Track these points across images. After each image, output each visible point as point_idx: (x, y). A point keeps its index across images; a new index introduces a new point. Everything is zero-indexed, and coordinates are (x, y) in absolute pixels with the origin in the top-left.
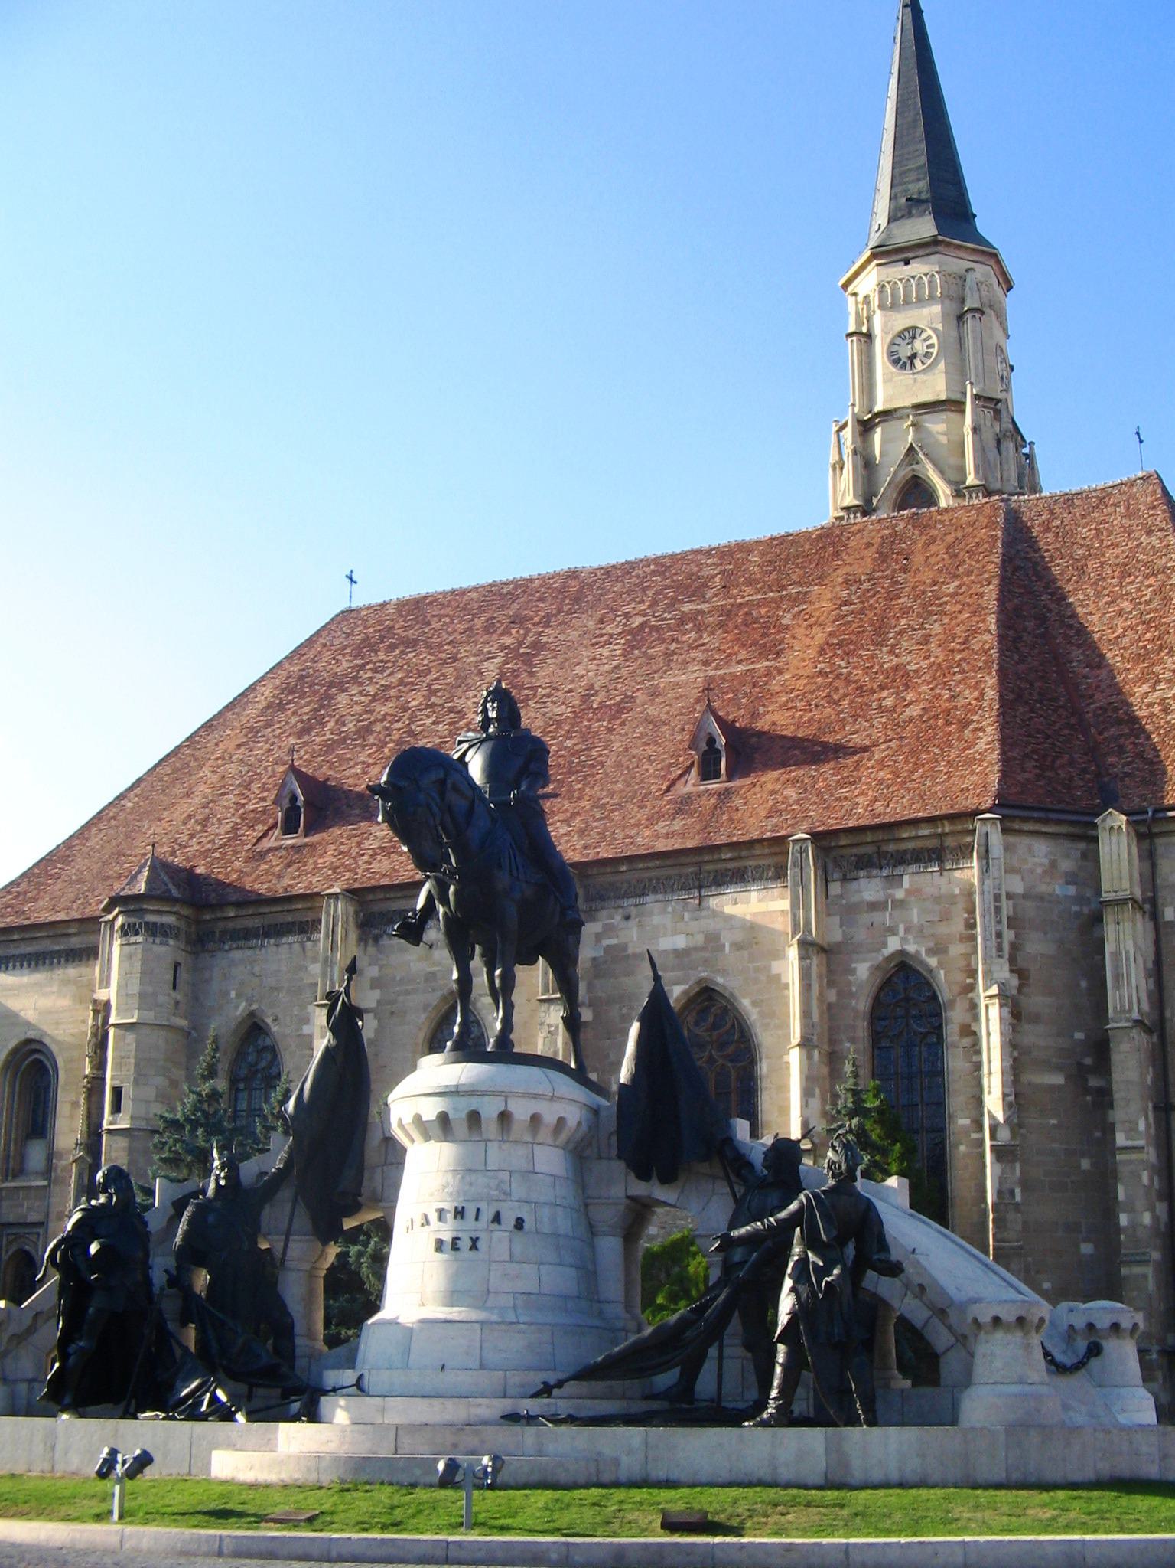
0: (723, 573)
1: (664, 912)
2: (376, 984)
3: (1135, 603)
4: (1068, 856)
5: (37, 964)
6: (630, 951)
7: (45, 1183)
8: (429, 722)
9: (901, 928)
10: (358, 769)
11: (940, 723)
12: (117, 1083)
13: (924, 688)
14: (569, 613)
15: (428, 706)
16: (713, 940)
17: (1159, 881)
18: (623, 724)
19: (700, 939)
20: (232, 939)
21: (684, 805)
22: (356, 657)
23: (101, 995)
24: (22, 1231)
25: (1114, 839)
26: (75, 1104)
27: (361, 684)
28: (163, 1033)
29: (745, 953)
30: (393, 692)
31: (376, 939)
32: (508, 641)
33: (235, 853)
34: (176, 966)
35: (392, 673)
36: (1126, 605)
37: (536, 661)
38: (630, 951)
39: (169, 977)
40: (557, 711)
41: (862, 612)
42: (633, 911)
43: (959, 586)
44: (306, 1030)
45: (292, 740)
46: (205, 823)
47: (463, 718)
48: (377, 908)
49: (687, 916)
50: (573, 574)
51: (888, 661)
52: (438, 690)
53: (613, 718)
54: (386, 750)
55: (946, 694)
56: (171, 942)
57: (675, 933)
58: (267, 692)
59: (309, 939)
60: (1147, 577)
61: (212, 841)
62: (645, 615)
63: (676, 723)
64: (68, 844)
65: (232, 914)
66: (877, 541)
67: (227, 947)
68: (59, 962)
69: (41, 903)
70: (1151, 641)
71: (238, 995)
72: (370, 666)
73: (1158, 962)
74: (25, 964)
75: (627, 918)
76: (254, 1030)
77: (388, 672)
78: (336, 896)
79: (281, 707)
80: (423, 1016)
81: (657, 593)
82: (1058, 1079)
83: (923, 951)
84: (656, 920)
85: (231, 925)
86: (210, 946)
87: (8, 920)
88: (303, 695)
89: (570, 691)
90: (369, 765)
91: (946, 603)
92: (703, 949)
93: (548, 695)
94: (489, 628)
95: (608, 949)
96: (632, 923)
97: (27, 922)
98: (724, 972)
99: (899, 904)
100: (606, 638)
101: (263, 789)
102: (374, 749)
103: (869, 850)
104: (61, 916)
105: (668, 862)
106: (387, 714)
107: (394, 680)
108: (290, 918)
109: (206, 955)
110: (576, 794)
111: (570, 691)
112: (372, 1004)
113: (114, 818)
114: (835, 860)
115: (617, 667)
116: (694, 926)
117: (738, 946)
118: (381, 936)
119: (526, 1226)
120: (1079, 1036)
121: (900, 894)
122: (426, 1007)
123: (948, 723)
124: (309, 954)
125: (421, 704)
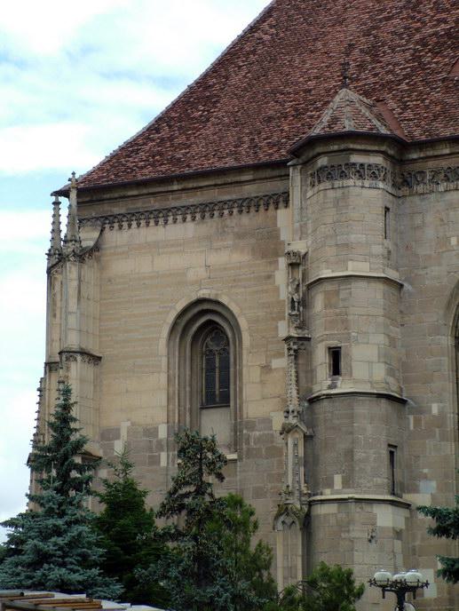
5: (203, 217)
12: (334, 343)
20: (447, 179)
23: (300, 246)
26: (266, 369)
28: (380, 286)
33: (426, 83)
34: (387, 209)
46: (374, 52)
56: (381, 185)
61: (391, 72)
65: (447, 151)
67: (441, 188)
68: (231, 213)
69: (195, 150)
74: (189, 217)
85: (444, 164)
86: (420, 188)
87: (163, 168)
97: (187, 171)
104: (230, 162)
109: (416, 199)
113: (254, 52)
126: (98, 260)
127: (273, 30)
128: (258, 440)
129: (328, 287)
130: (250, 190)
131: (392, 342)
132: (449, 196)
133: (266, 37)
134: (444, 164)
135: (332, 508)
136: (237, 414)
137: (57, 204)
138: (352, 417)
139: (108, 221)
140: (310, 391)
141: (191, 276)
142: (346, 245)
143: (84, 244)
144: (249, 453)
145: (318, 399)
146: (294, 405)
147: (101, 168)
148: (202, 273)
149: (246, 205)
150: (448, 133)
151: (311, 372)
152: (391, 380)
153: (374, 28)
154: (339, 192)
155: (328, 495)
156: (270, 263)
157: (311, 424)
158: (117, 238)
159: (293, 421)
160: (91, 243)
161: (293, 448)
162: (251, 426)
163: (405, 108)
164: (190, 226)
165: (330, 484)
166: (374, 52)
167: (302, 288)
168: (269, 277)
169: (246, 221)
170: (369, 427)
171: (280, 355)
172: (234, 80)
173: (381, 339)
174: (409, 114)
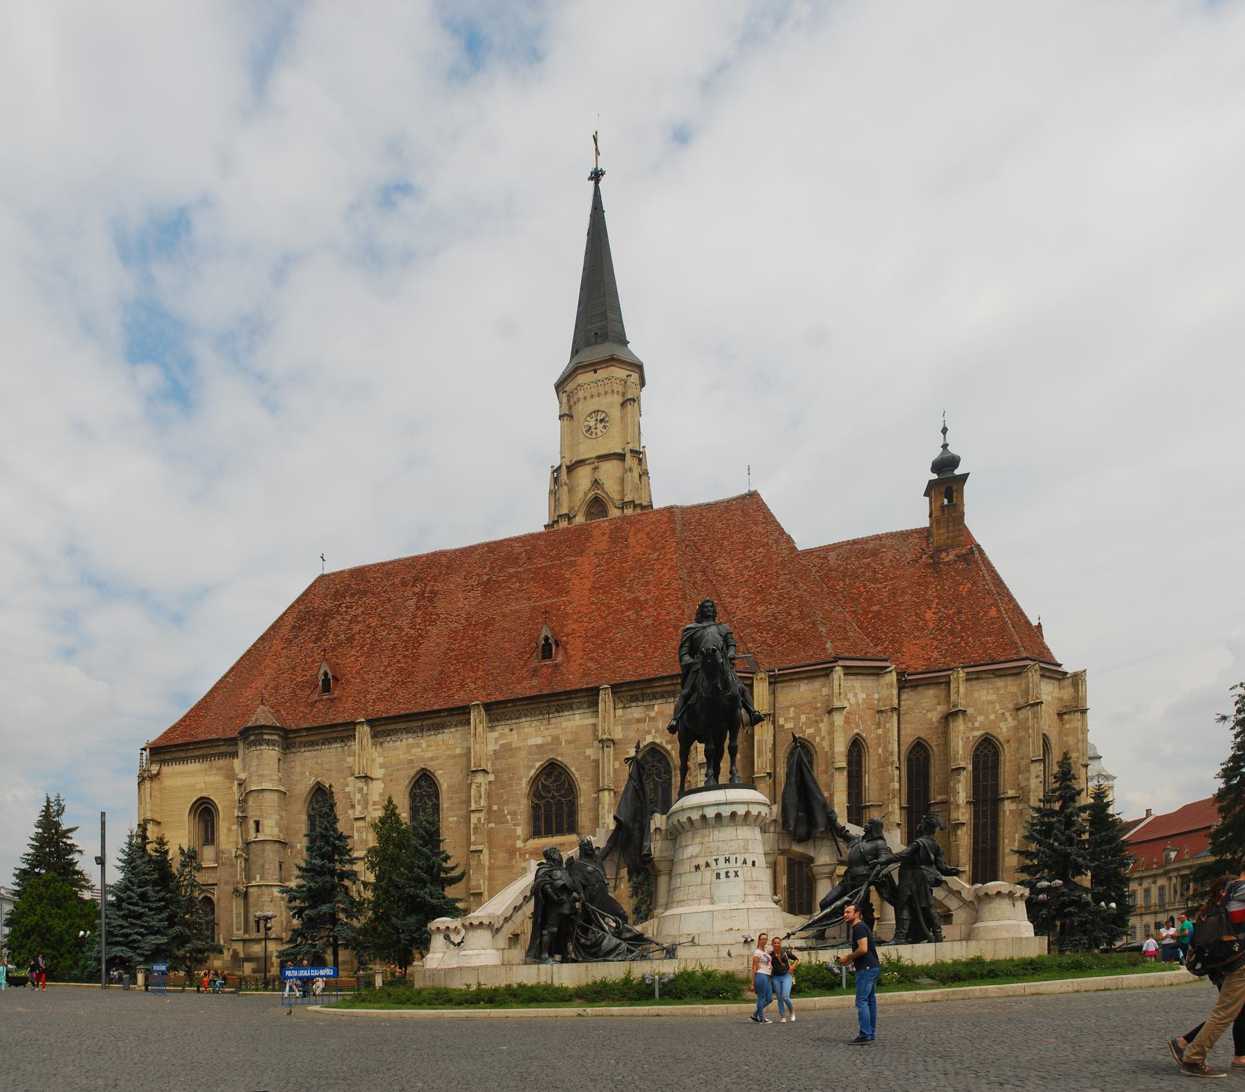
1: (530, 726)
2: (382, 766)
3: (754, 562)
6: (513, 746)
8: (384, 633)
9: (653, 731)
10: (353, 659)
12: (257, 819)
13: (651, 609)
15: (382, 626)
16: (556, 740)
18: (491, 632)
19: (549, 739)
20: (305, 746)
21: (535, 672)
22: (334, 601)
23: (243, 776)
26: (229, 830)
27: (342, 615)
29: (573, 745)
30: (360, 619)
31: (381, 744)
34: (279, 760)
36: (749, 563)
38: (513, 746)
39: (277, 766)
42: (514, 726)
44: (347, 789)
45: (312, 645)
47: (402, 631)
49: (542, 728)
52: (386, 617)
53: (486, 629)
55: (664, 612)
57: (536, 737)
58: (290, 620)
59: (346, 745)
60: (759, 548)
61: (283, 698)
71: (310, 774)
75: (511, 730)
77: (355, 608)
79: (301, 628)
83: (664, 742)
84: (526, 730)
86: (294, 750)
88: (310, 621)
90: (358, 657)
91: (654, 564)
95: (502, 745)
96: (513, 732)
98: (562, 755)
99: (653, 719)
101: (303, 670)
102: (358, 648)
104: (214, 736)
105: (534, 701)
108: (335, 735)
109: (292, 755)
110: (475, 669)
112: (382, 776)
113: (225, 687)
114: (619, 698)
116: (546, 733)
117: (568, 742)
118: (383, 742)
121: (653, 714)
122: (408, 777)
124: (346, 752)
125: (377, 624)
126: (159, 779)
129: (254, 794)
130: (223, 749)
131: (282, 818)
132: (305, 754)
133: (231, 681)
134: (304, 739)
137: (141, 754)
138: (264, 850)
139: (163, 762)
140: (247, 839)
141: (198, 787)
142: (262, 775)
143: (153, 772)
145: (250, 843)
146: (240, 846)
147: (160, 738)
148: (203, 786)
149: (221, 755)
150: (304, 726)
151: (247, 831)
152: (280, 834)
153: (276, 677)
157: (248, 854)
158: (167, 769)
159: (240, 852)
160: (156, 772)
161: (240, 864)
163: (288, 714)
164: (198, 764)
166: (276, 689)
167: (244, 795)
168: (231, 788)
169: (222, 762)
170: (271, 855)
171: (234, 824)
172: (217, 700)
173: (277, 817)
174: (290, 717)
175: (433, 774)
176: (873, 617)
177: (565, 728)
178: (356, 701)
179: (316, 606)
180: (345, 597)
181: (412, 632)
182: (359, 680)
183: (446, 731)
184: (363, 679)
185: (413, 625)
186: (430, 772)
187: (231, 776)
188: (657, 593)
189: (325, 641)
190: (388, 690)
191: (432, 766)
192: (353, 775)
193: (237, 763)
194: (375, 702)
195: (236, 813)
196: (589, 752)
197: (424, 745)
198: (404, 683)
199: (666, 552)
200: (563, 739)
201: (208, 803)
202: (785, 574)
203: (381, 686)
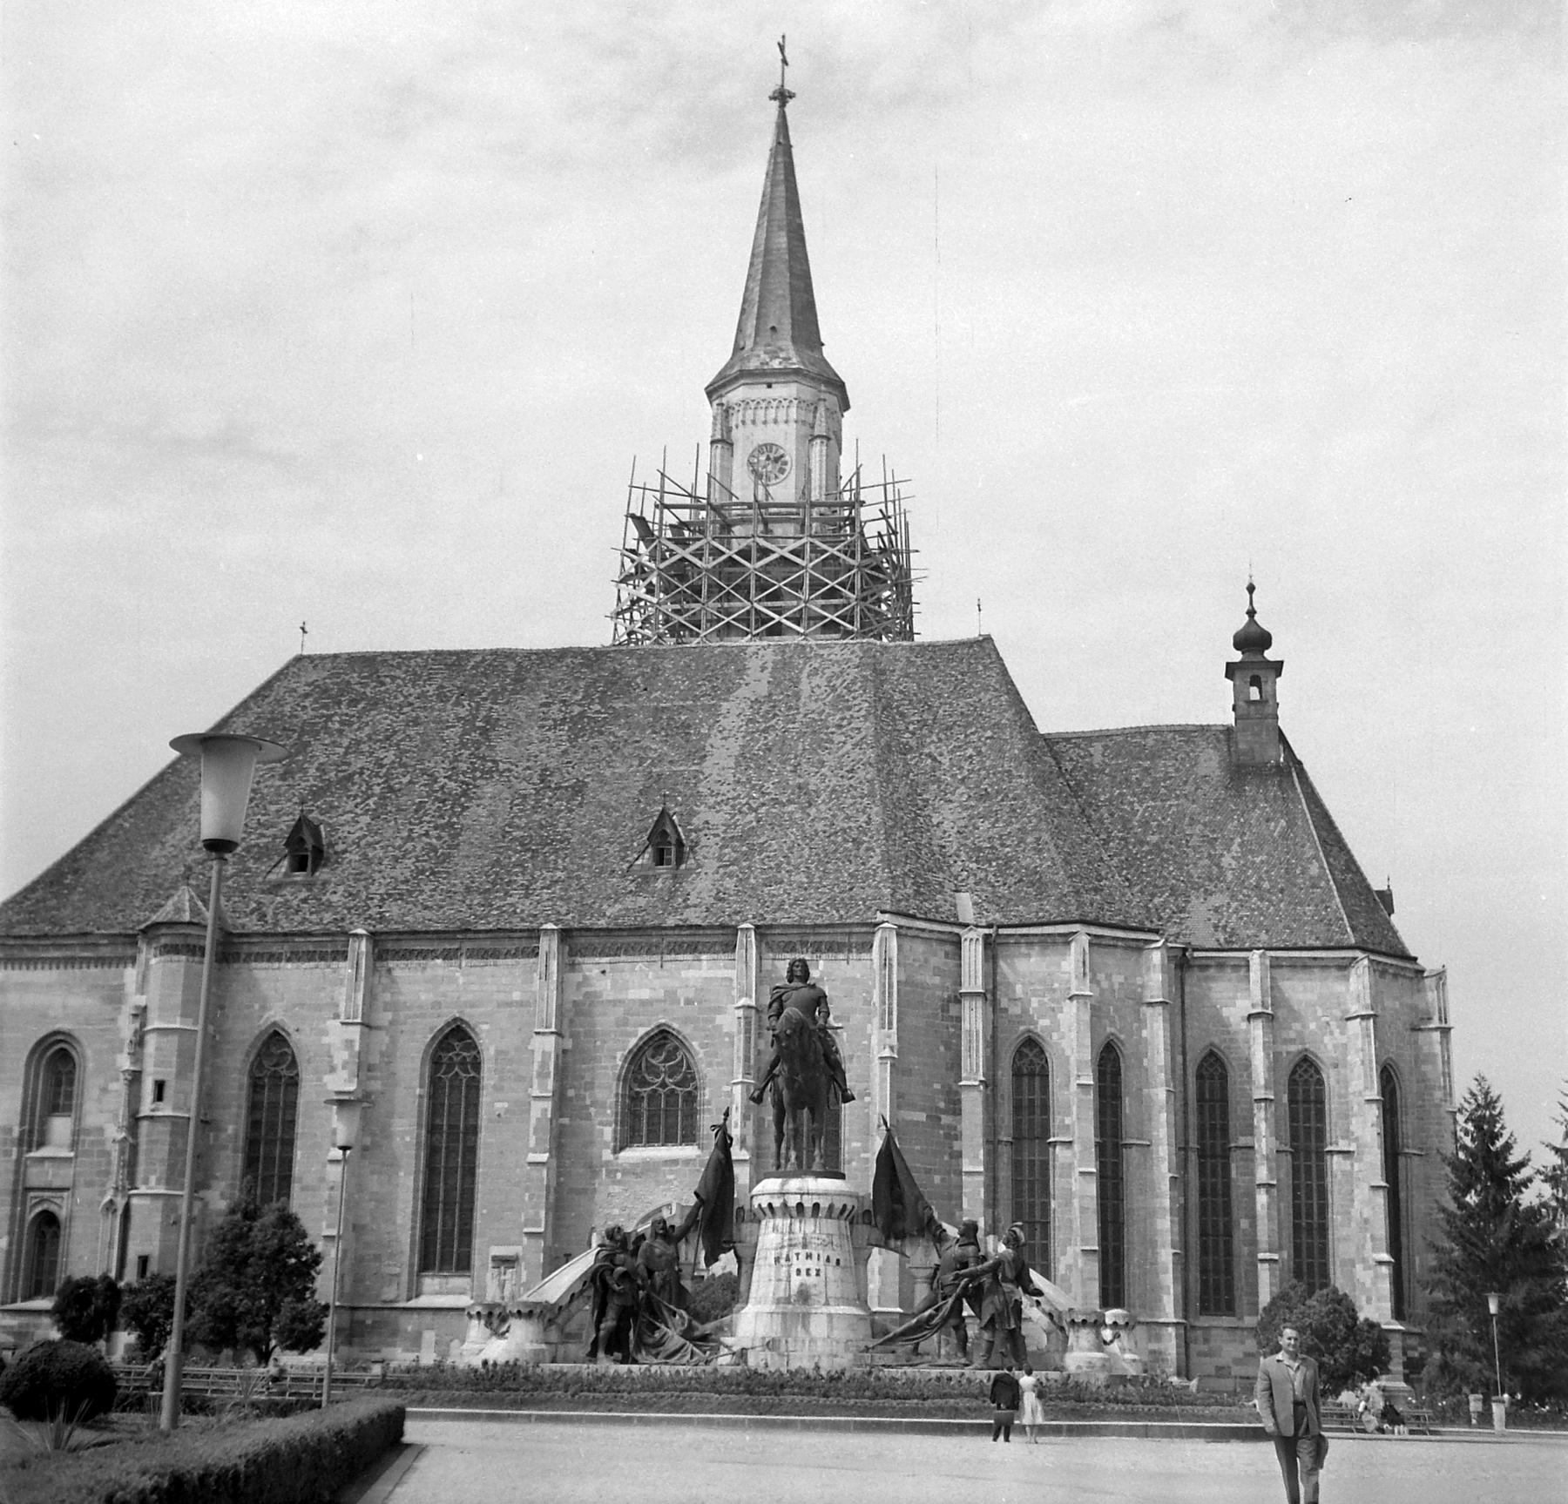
0: (643, 674)
4: (935, 955)
6: (605, 997)
7: (72, 1154)
8: (405, 780)
11: (840, 839)
12: (160, 1078)
13: (823, 807)
14: (514, 692)
16: (671, 996)
17: (998, 978)
19: (661, 994)
24: (47, 1194)
25: (973, 947)
27: (331, 735)
30: (365, 748)
32: (463, 712)
35: (359, 728)
37: (492, 734)
40: (518, 786)
41: (765, 730)
43: (843, 719)
44: (325, 1040)
48: (390, 946)
50: (509, 655)
51: (794, 781)
54: (371, 802)
57: (640, 987)
59: (329, 967)
62: (580, 705)
63: (627, 811)
64: (73, 856)
66: (770, 665)
70: (990, 785)
72: (337, 718)
73: (994, 1037)
76: (275, 1040)
77: (355, 726)
78: (362, 935)
80: (431, 1036)
81: (587, 687)
82: (922, 1117)
89: (528, 768)
92: (665, 1001)
93: (509, 770)
94: (442, 697)
95: (587, 993)
100: (551, 722)
102: (359, 800)
103: (796, 939)
106: (362, 768)
107: (362, 735)
111: (528, 768)
114: (767, 943)
115: (565, 752)
116: (657, 982)
119: (842, 1263)
120: (937, 1086)
122: (431, 1029)
123: (846, 841)
125: (393, 762)
127: (132, 820)
128: (92, 1143)
135: (147, 1201)
136: (78, 1120)
144: (87, 1153)
154: (174, 965)
155: (143, 1190)
156: (116, 1009)
162: (88, 1132)
165: (146, 1182)
168: (113, 1020)
175: (473, 1030)
176: (1150, 852)
177: (688, 979)
178: (350, 894)
179: (287, 709)
180: (339, 703)
181: (452, 785)
182: (357, 858)
183: (500, 962)
184: (365, 856)
185: (453, 774)
186: (466, 1023)
187: (115, 996)
188: (834, 782)
189: (301, 778)
190: (406, 881)
191: (470, 1015)
192: (337, 1016)
193: (130, 974)
194: (383, 900)
195: (125, 1062)
196: (719, 1019)
197: (461, 981)
198: (433, 873)
199: (852, 716)
200: (682, 995)
201: (66, 1042)
202: (1020, 777)
203: (395, 873)
